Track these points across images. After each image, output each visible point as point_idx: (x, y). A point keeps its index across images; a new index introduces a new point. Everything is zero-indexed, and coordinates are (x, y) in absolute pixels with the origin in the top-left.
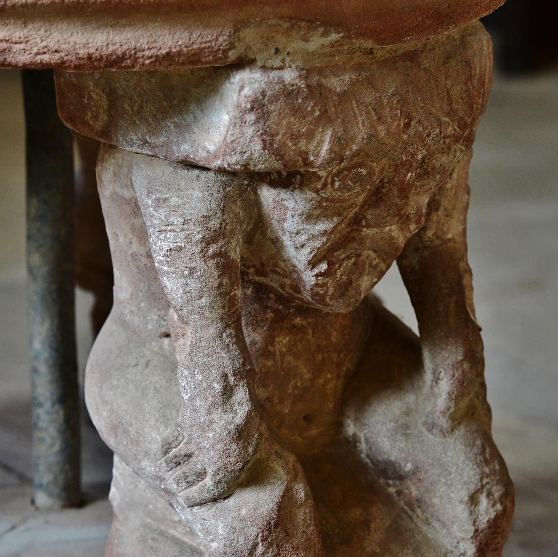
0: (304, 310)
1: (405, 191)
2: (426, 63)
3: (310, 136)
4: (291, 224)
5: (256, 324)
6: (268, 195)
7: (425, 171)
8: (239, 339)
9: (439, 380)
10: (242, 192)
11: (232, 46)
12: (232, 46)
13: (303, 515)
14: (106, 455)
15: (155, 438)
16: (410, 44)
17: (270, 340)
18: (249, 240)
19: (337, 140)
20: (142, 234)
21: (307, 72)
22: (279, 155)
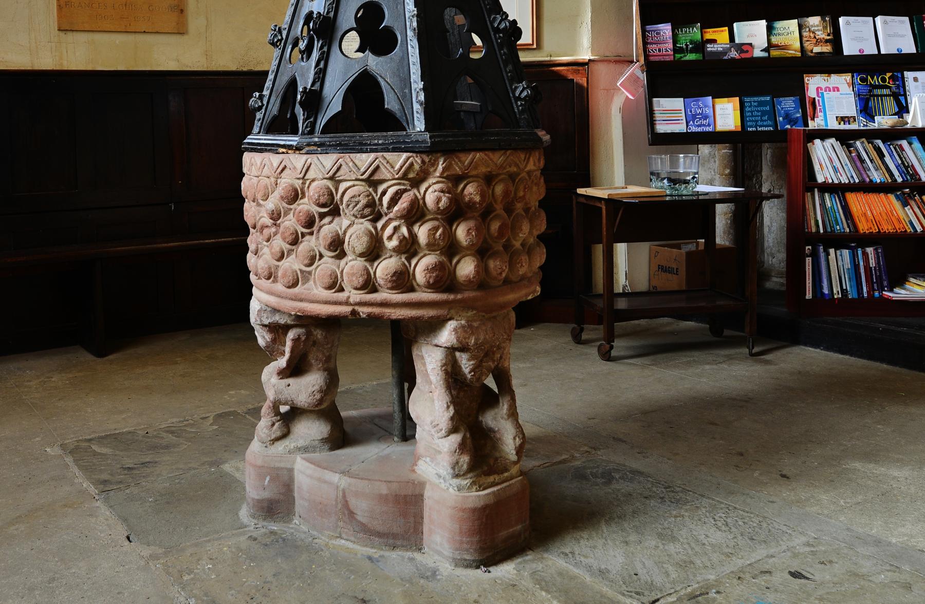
0: (468, 385)
1: (494, 353)
4: (464, 362)
5: (455, 389)
6: (458, 354)
7: (499, 348)
8: (451, 393)
9: (504, 407)
10: (451, 353)
14: (414, 426)
15: (428, 420)
16: (494, 314)
17: (458, 393)
18: (453, 366)
19: (476, 339)
20: (424, 364)
21: (468, 321)
22: (461, 343)
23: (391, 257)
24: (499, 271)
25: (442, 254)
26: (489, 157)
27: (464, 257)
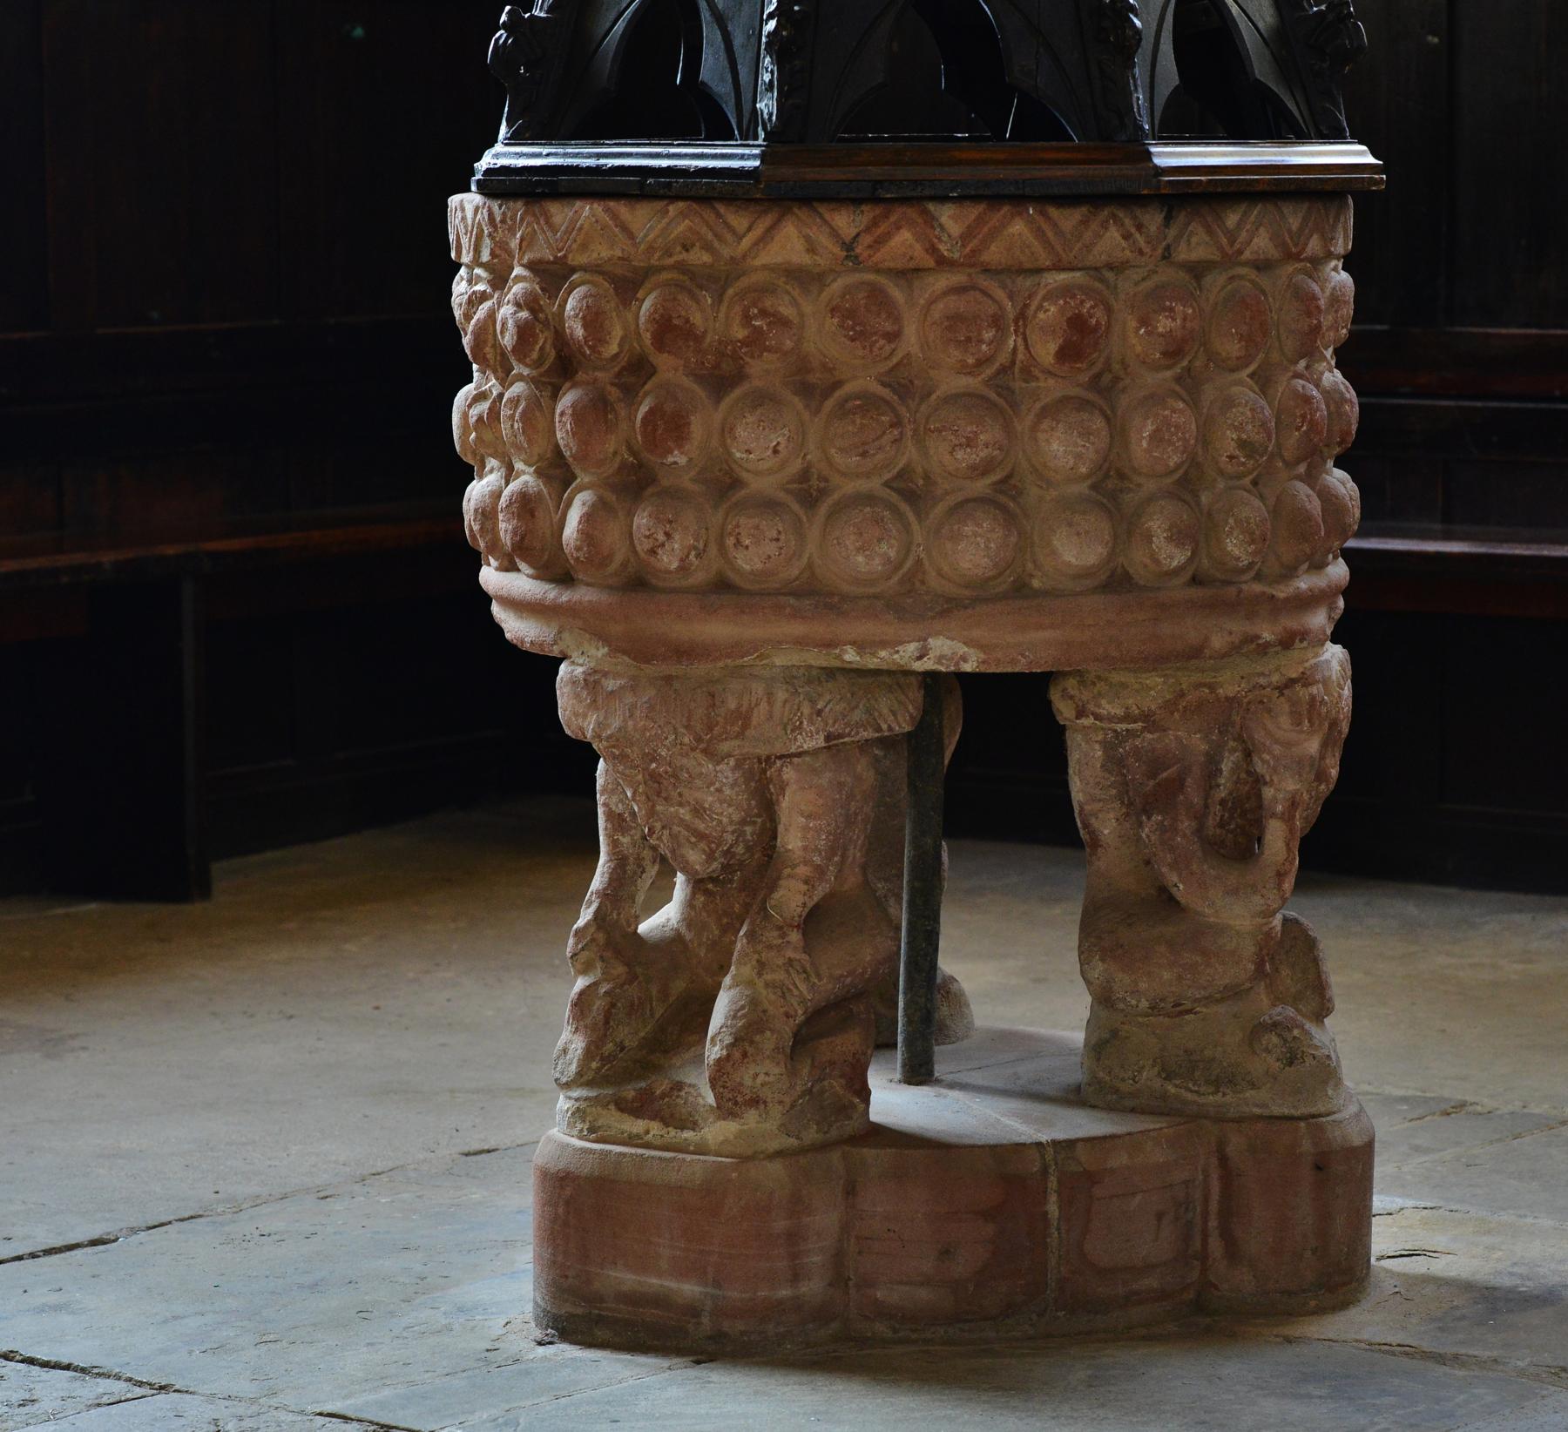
2: (676, 685)
3: (585, 716)
11: (555, 643)
12: (555, 643)
13: (599, 1004)
19: (599, 724)
23: (491, 471)
24: (647, 545)
25: (539, 473)
26: (615, 217)
27: (580, 489)
